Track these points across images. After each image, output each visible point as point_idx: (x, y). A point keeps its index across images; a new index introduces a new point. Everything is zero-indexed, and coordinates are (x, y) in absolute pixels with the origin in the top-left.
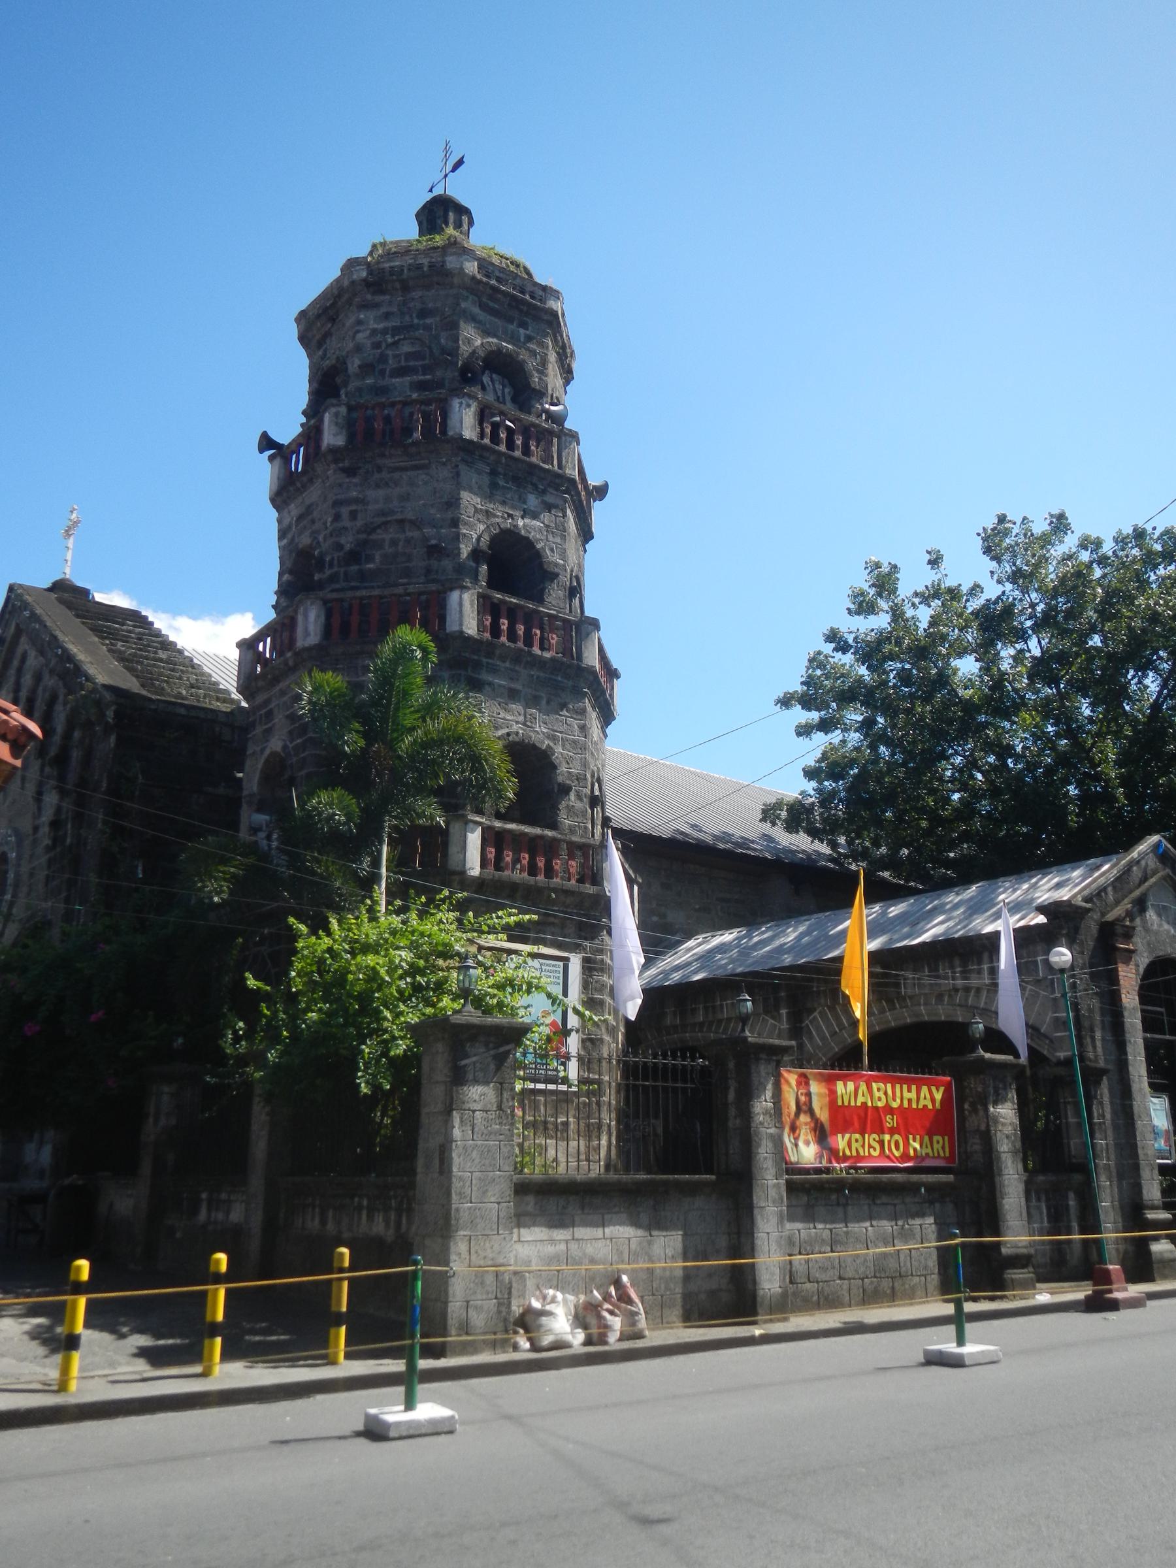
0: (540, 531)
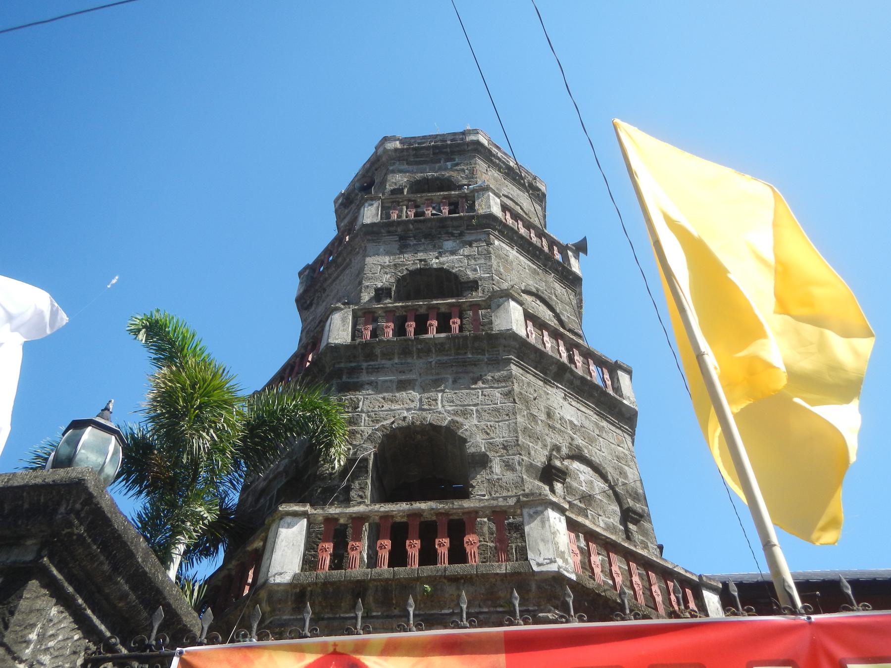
0: (460, 261)
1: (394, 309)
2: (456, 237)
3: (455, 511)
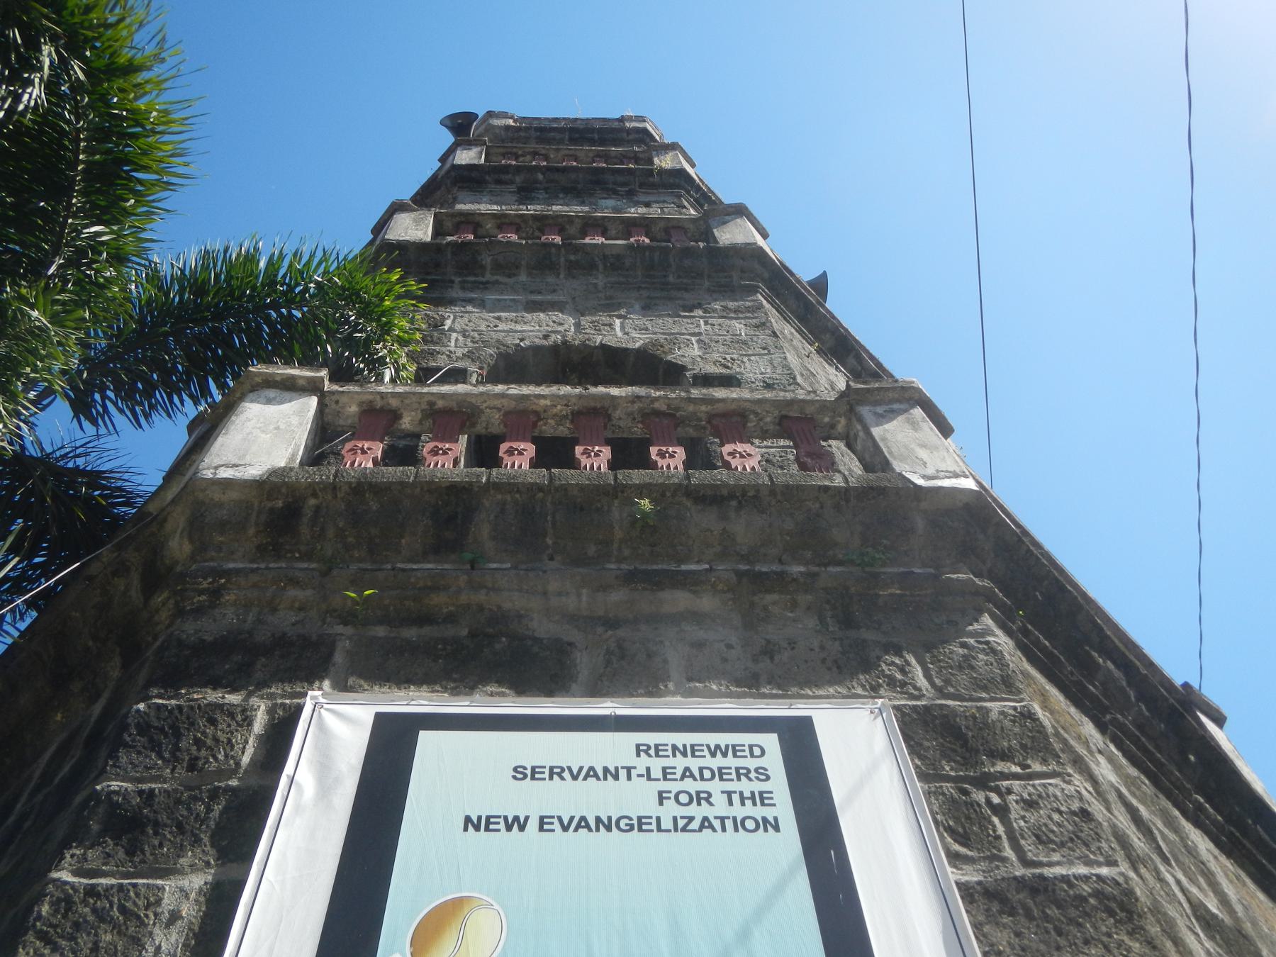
1: (518, 221)
2: (622, 195)
3: (691, 408)
